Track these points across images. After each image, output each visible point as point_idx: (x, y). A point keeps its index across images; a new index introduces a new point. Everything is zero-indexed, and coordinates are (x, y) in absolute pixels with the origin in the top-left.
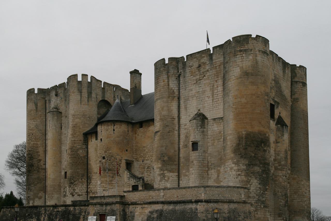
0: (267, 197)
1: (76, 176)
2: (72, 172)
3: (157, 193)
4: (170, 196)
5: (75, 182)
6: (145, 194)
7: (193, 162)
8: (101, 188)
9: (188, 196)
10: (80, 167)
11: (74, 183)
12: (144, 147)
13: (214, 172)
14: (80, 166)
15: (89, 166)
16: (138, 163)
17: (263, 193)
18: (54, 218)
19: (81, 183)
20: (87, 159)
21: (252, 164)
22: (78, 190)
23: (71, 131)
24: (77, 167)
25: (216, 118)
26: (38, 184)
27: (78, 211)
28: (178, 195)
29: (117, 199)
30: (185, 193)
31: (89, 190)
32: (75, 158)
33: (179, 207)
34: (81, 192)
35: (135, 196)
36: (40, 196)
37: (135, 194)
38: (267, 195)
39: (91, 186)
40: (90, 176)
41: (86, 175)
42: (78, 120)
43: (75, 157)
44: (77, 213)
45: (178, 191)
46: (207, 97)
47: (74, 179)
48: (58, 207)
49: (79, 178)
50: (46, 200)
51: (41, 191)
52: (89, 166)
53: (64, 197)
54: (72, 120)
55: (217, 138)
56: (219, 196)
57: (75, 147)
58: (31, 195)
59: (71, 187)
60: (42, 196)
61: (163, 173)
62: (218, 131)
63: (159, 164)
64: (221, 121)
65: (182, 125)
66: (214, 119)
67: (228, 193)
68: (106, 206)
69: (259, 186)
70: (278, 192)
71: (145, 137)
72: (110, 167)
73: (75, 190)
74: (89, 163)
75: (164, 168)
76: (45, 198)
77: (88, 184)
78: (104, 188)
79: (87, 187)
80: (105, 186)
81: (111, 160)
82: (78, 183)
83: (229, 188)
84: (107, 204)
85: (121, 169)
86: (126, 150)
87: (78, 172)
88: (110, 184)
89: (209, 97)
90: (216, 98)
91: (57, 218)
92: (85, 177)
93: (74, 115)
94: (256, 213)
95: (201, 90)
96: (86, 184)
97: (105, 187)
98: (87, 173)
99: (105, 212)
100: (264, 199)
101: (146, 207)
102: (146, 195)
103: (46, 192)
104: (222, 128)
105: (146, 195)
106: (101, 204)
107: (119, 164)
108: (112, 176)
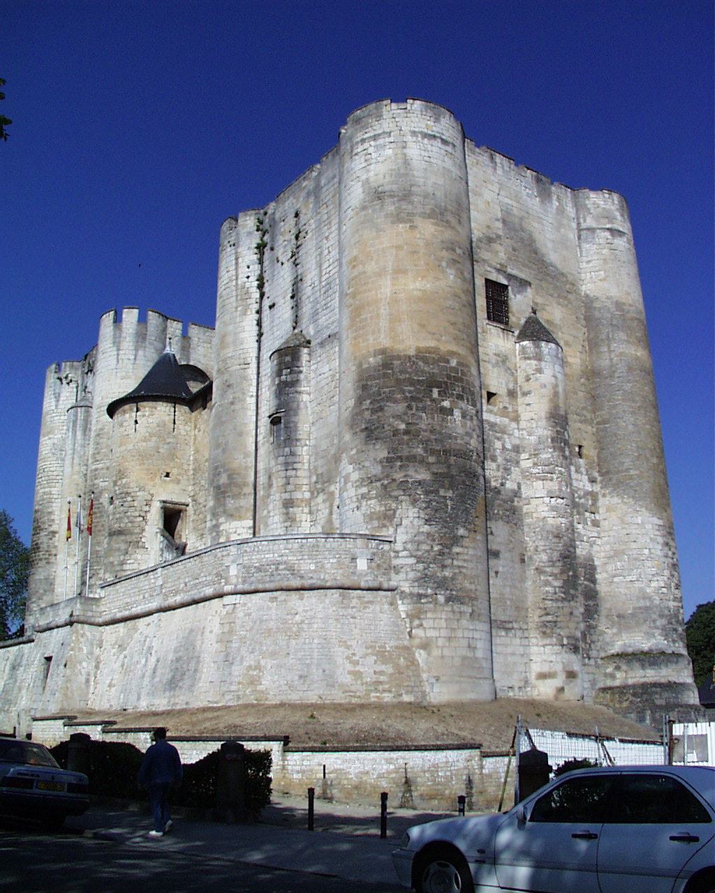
0: (459, 567)
17: (441, 553)
21: (400, 458)
38: (460, 557)
56: (277, 569)
67: (306, 557)
69: (426, 528)
70: (537, 551)
81: (126, 504)
83: (309, 540)
85: (147, 527)
86: (165, 474)
87: (97, 551)
94: (416, 622)
100: (447, 573)
104: (337, 364)
107: (143, 514)
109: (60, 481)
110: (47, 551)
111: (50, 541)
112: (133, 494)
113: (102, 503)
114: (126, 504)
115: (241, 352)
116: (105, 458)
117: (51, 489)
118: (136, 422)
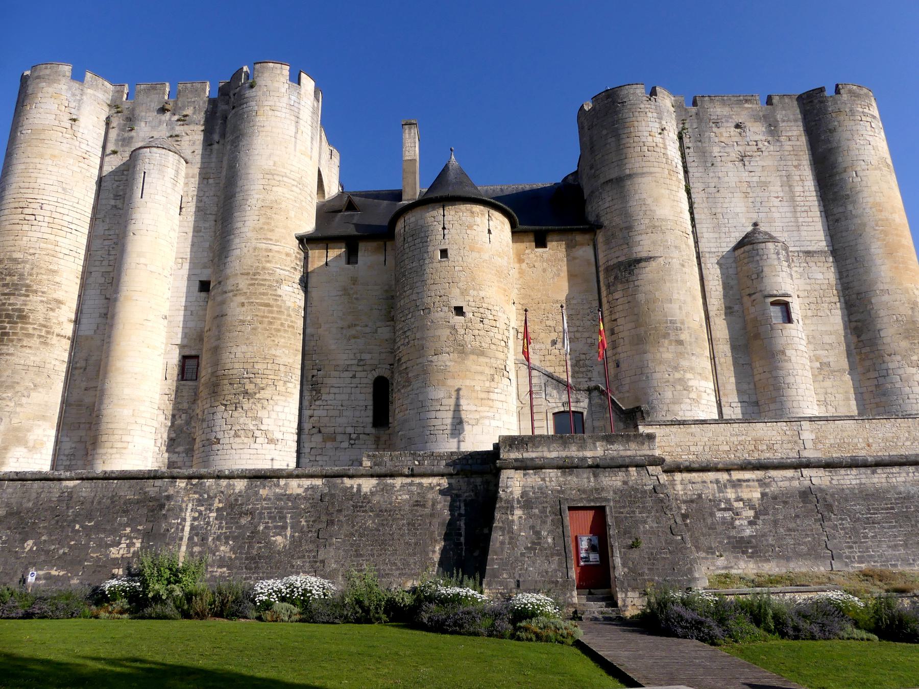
1: (266, 372)
5: (262, 392)
10: (283, 340)
11: (257, 396)
13: (833, 386)
14: (284, 337)
19: (283, 398)
24: (272, 339)
25: (815, 252)
28: (871, 441)
29: (646, 446)
32: (266, 309)
34: (282, 429)
35: (691, 438)
36: (35, 437)
46: (777, 197)
47: (258, 381)
48: (279, 478)
49: (276, 378)
55: (827, 299)
57: (271, 272)
60: (45, 439)
65: (707, 255)
68: (595, 476)
72: (483, 344)
82: (274, 398)
84: (597, 467)
87: (274, 355)
89: (780, 199)
90: (802, 204)
91: (284, 528)
95: (755, 179)
101: (748, 481)
102: (740, 438)
106: (566, 467)
108: (489, 373)
109: (74, 232)
110: (45, 326)
111: (51, 314)
112: (494, 313)
113: (280, 296)
115: (682, 220)
117: (58, 238)
118: (489, 232)
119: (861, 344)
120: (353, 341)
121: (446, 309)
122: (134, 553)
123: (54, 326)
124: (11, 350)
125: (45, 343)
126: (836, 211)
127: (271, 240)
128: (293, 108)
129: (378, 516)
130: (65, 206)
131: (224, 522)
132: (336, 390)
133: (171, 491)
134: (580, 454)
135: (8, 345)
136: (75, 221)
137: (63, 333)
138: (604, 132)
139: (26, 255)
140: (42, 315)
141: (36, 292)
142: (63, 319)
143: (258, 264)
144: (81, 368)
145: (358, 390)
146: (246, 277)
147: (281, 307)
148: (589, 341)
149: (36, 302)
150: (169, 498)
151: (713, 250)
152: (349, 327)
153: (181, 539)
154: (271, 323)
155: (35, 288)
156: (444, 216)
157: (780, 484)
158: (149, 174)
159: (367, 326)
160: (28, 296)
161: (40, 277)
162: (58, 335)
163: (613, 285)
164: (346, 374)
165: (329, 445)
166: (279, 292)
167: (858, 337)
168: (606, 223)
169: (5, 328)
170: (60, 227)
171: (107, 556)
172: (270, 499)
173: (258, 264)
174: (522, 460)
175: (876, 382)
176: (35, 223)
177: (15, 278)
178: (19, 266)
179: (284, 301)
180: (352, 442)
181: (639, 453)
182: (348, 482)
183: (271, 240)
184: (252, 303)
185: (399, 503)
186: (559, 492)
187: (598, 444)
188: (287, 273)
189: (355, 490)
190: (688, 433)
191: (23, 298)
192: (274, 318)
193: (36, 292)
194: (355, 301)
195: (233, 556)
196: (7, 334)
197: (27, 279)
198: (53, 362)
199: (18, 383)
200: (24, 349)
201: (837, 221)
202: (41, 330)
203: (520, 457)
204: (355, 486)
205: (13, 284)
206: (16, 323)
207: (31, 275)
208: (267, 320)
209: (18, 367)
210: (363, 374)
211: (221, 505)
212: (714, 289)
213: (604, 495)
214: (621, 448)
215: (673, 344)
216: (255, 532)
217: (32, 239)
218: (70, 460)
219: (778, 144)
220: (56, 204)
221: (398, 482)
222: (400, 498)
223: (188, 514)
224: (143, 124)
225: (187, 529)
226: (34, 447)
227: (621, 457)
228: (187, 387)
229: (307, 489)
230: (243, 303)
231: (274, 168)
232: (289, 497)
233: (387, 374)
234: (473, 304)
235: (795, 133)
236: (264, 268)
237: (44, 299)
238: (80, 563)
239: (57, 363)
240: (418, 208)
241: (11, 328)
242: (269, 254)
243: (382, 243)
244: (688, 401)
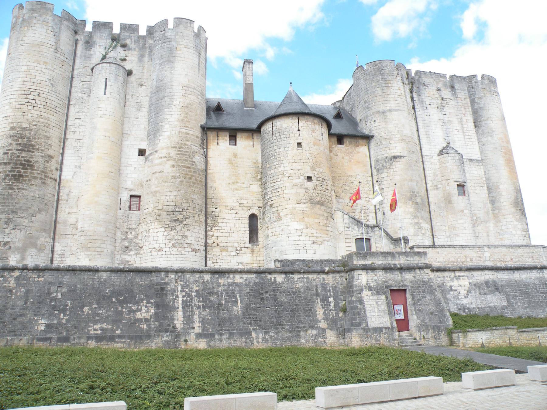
2: (179, 197)
3: (479, 253)
4: (499, 257)
5: (187, 220)
6: (458, 253)
7: (463, 211)
8: (308, 238)
9: (527, 259)
10: (197, 189)
11: (184, 223)
12: (350, 176)
15: (210, 192)
16: (340, 201)
18: (223, 301)
20: (206, 176)
22: (192, 238)
23: (180, 113)
25: (473, 160)
26: (40, 213)
27: (301, 285)
29: (423, 258)
30: (521, 255)
31: (209, 242)
32: (187, 169)
33: (517, 276)
37: (438, 253)
39: (216, 234)
40: (213, 212)
41: (204, 209)
42: (195, 98)
43: (188, 167)
44: (302, 290)
45: (511, 250)
46: (456, 130)
49: (194, 212)
50: (55, 256)
51: (44, 230)
52: (212, 192)
53: (125, 252)
54: (181, 94)
58: (14, 240)
59: (175, 229)
60: (46, 244)
61: (417, 223)
62: (479, 176)
63: (408, 206)
64: (481, 164)
65: (426, 157)
66: (471, 160)
68: (401, 273)
71: (350, 161)
72: (323, 199)
73: (186, 237)
74: (210, 184)
75: (419, 215)
76: (53, 252)
77: (209, 228)
78: (314, 239)
79: (206, 235)
80: (315, 235)
82: (194, 224)
84: (402, 269)
88: (325, 232)
90: (467, 134)
92: (204, 212)
93: (188, 86)
96: (204, 227)
97: (317, 237)
98: (206, 204)
99: (406, 286)
101: (463, 276)
103: (57, 237)
105: (459, 255)
106: (387, 269)
109: (58, 112)
110: (44, 172)
114: (323, 186)
116: (195, 128)
117: (49, 116)
119: (494, 208)
120: (236, 192)
121: (302, 178)
122: (151, 316)
123: (49, 172)
124: (25, 187)
125: (44, 183)
126: (483, 140)
127: (188, 127)
128: (197, 48)
129: (287, 295)
130: (53, 95)
131: (201, 299)
132: (227, 221)
133: (167, 280)
134: (393, 262)
135: (23, 183)
136: (59, 106)
137: (53, 177)
138: (374, 84)
139: (31, 125)
140: (42, 165)
141: (38, 149)
142: (53, 168)
143: (182, 142)
144: (65, 200)
145: (240, 221)
146: (175, 149)
147: (195, 169)
148: (367, 199)
149: (38, 156)
150: (166, 284)
151: (428, 154)
152: (233, 183)
153: (178, 308)
154: (190, 179)
155: (37, 147)
156: (299, 123)
157: (476, 278)
158: (109, 80)
159: (243, 183)
160: (33, 152)
161: (40, 140)
162: (51, 178)
163: (381, 170)
164: (232, 211)
165: (224, 253)
166: (194, 160)
167: (493, 205)
168: (376, 135)
169: (20, 172)
170: (50, 109)
171: (134, 317)
172: (226, 285)
173: (182, 142)
174: (366, 265)
175: (501, 228)
176: (36, 105)
177: (25, 140)
178: (27, 132)
179: (196, 165)
180: (238, 252)
181: (420, 262)
182: (269, 276)
183: (188, 127)
184: (179, 165)
185: (298, 288)
186: (384, 281)
187: (401, 256)
188: (197, 148)
189: (273, 281)
190: (437, 252)
191: (31, 153)
192: (192, 176)
193: (38, 149)
194: (236, 168)
195: (210, 318)
196: (22, 176)
197: (32, 141)
198: (49, 195)
199: (30, 208)
200: (32, 186)
201: (483, 145)
202: (42, 174)
203: (364, 263)
204: (273, 278)
205: (24, 144)
206: (27, 169)
207: (35, 138)
208: (188, 176)
209: (30, 198)
210: (243, 212)
211: (197, 288)
212: (429, 175)
213: (405, 283)
214: (412, 259)
215: (414, 204)
216: (220, 305)
217: (34, 115)
218: (62, 258)
219: (456, 101)
220: (48, 94)
221: (296, 277)
222: (298, 285)
223: (179, 293)
224: (98, 47)
225: (180, 302)
226: (40, 249)
227: (412, 264)
228: (134, 215)
229: (246, 280)
230: (174, 165)
231: (189, 83)
232: (237, 284)
233: (257, 213)
234: (317, 176)
235: (464, 97)
236: (185, 144)
237: (43, 155)
238: (120, 321)
239: (50, 196)
240: (283, 117)
241: (24, 172)
242: (188, 136)
243: (251, 134)
244: (421, 234)
